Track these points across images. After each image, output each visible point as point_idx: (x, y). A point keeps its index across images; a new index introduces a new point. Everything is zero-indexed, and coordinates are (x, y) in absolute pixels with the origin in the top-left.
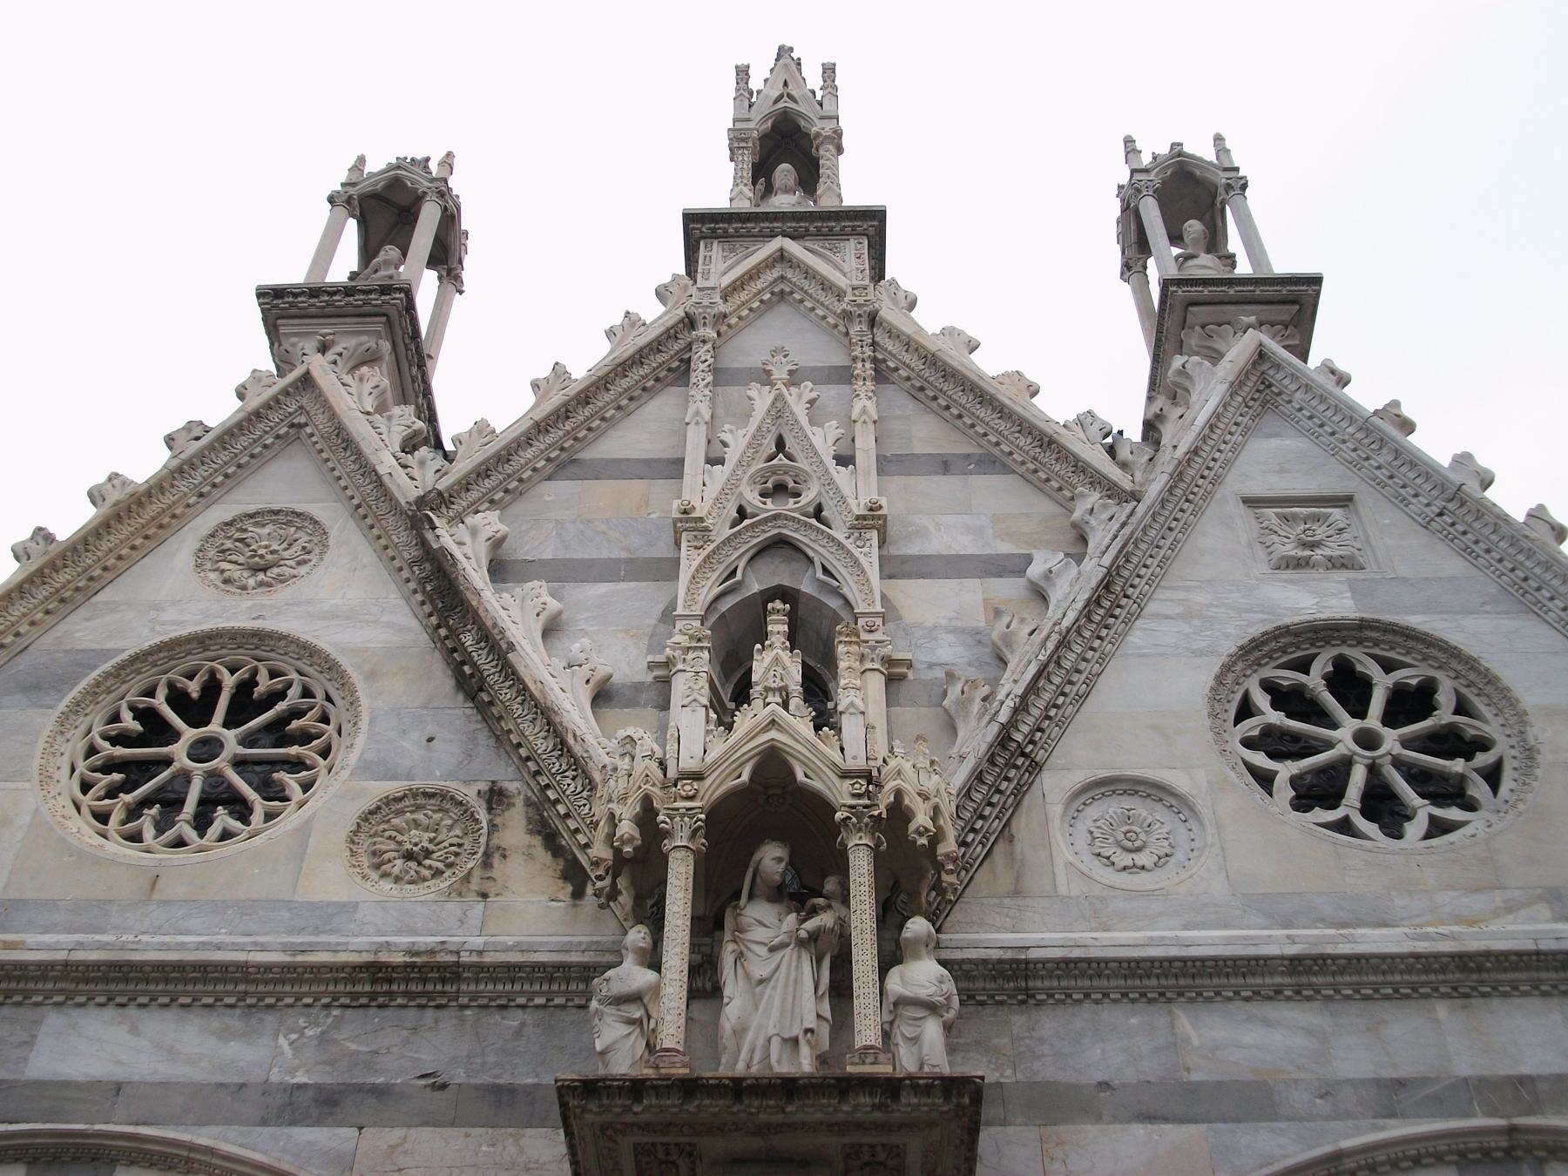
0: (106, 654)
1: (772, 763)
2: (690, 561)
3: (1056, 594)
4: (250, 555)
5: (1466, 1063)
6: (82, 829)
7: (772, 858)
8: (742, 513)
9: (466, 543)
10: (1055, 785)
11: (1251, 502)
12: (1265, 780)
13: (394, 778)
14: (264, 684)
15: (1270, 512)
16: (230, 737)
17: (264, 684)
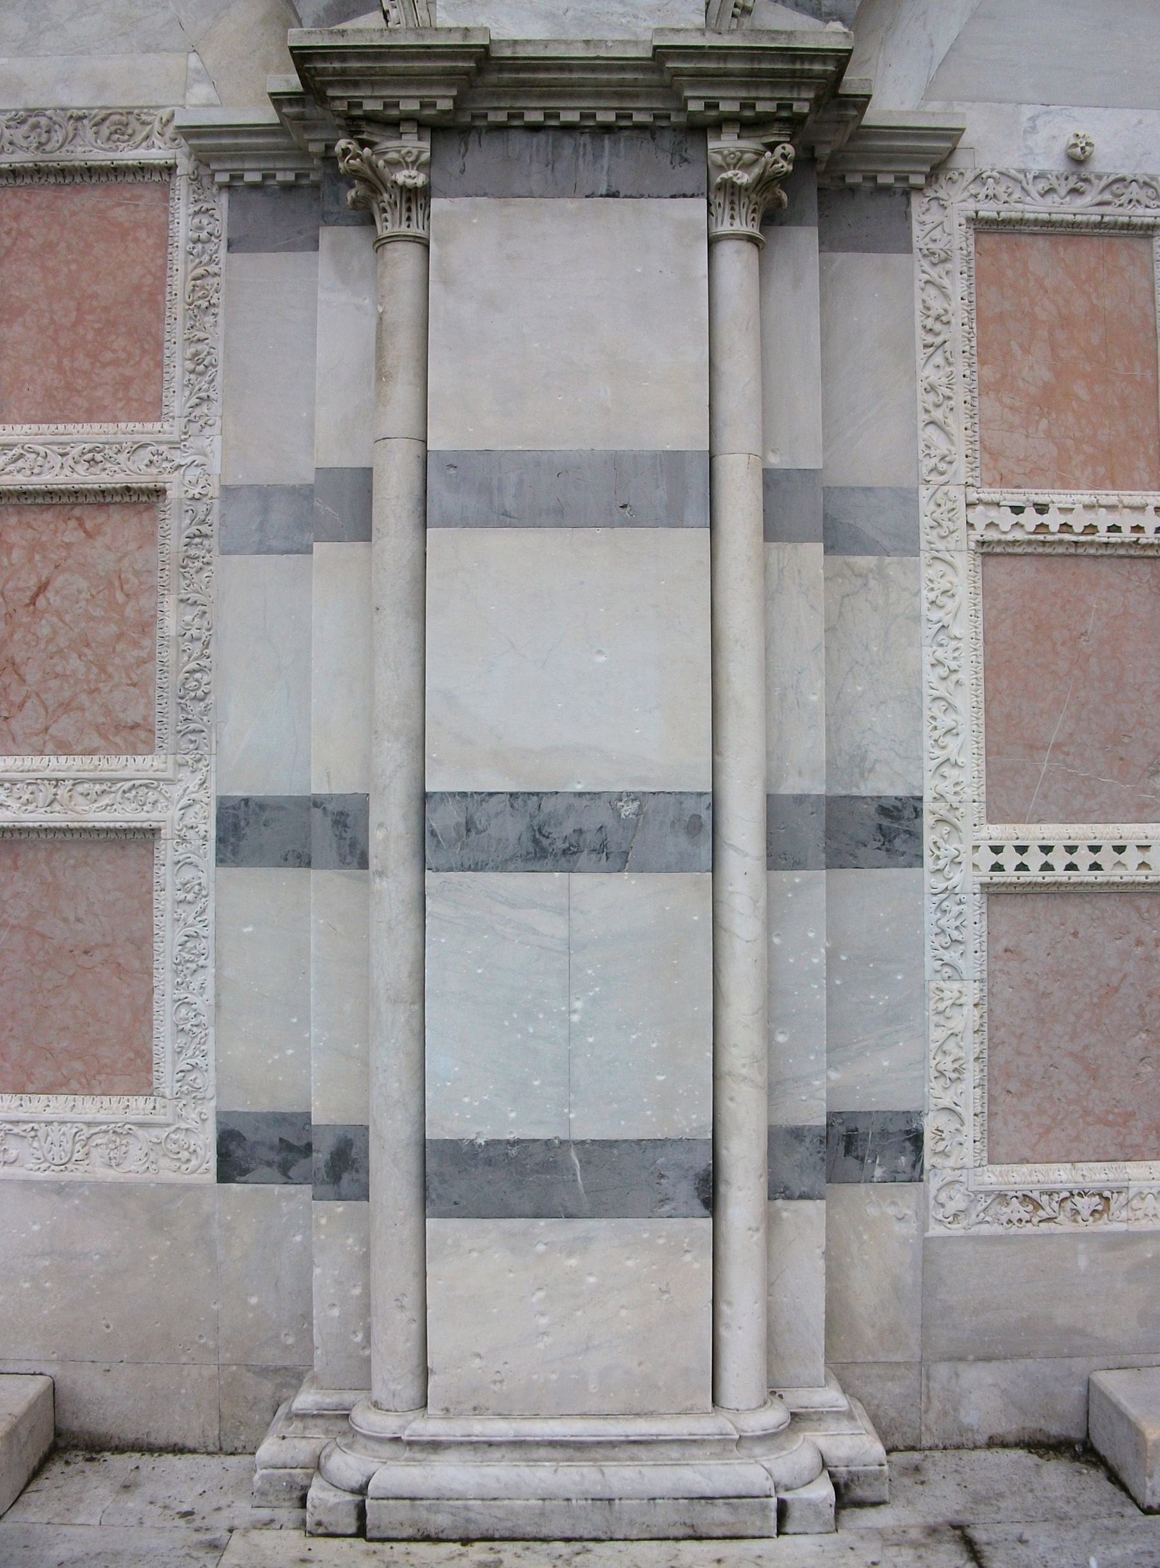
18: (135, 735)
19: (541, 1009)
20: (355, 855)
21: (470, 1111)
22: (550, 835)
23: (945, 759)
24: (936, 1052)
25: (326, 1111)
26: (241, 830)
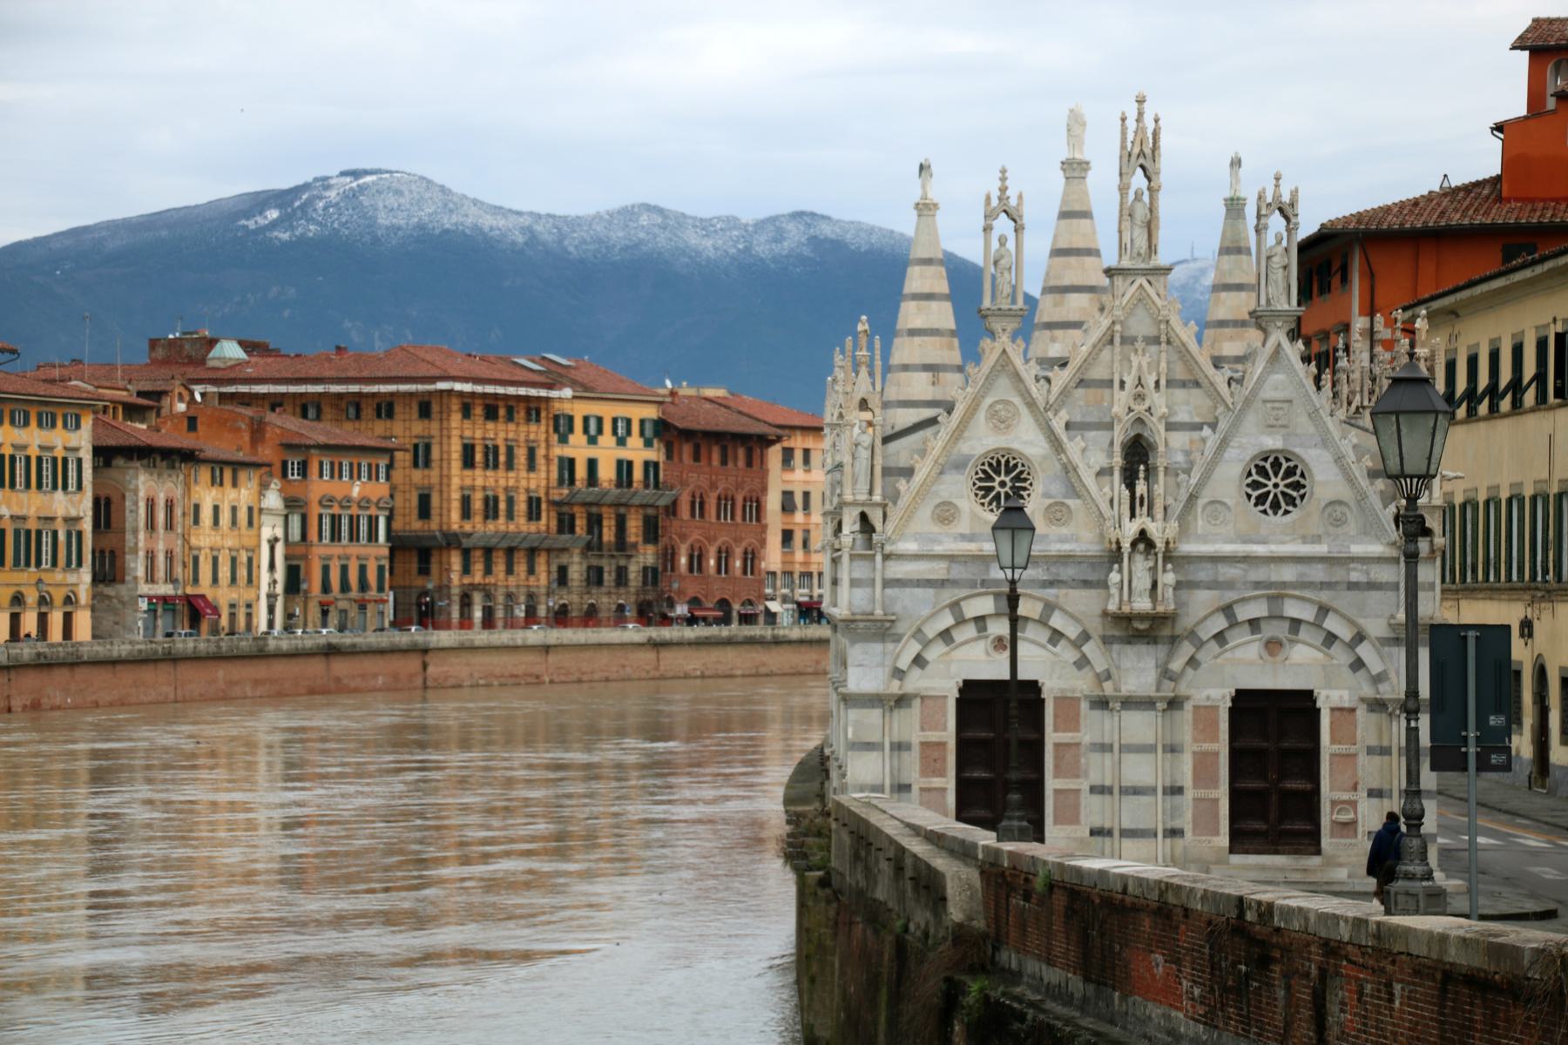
1: (1143, 533)
2: (1117, 428)
3: (1209, 444)
4: (1001, 421)
5: (1273, 579)
7: (1141, 547)
8: (1130, 410)
9: (1058, 424)
10: (1201, 502)
11: (1265, 401)
12: (1249, 496)
14: (1012, 463)
17: (1012, 463)
18: (1077, 776)
19: (1133, 812)
20: (1111, 793)
21: (1126, 824)
22: (1136, 791)
23: (1187, 780)
24: (1186, 821)
25: (1107, 825)
26: (1093, 790)
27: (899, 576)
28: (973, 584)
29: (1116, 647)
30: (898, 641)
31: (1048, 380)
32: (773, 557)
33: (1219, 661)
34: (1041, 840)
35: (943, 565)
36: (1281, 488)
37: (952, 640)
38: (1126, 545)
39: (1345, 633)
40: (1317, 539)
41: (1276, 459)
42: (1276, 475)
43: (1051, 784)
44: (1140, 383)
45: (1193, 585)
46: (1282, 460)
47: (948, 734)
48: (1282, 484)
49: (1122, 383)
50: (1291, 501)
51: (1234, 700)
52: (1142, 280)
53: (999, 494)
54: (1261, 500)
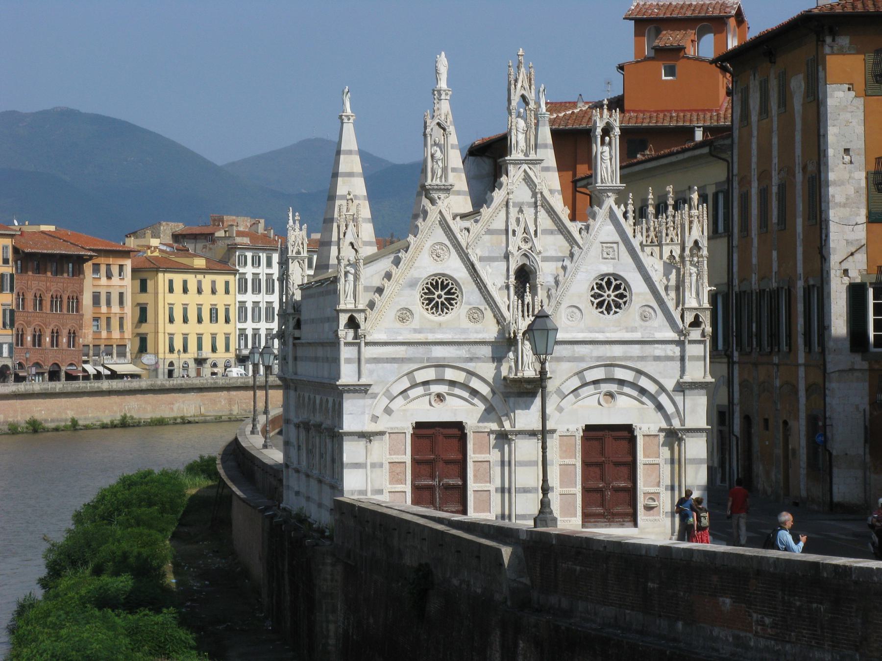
0: (420, 279)
5: (608, 355)
6: (425, 312)
8: (519, 249)
13: (470, 304)
15: (604, 245)
16: (443, 293)
27: (375, 356)
28: (421, 360)
29: (512, 400)
30: (375, 397)
31: (468, 230)
32: (87, 336)
33: (575, 406)
34: (636, 525)
35: (403, 348)
36: (612, 297)
37: (408, 397)
38: (520, 336)
39: (652, 388)
40: (634, 330)
41: (609, 279)
42: (609, 289)
43: (472, 486)
44: (526, 231)
45: (559, 359)
46: (613, 280)
47: (408, 458)
48: (613, 294)
49: (514, 232)
50: (618, 306)
51: (583, 431)
52: (525, 167)
53: (437, 302)
54: (600, 305)
